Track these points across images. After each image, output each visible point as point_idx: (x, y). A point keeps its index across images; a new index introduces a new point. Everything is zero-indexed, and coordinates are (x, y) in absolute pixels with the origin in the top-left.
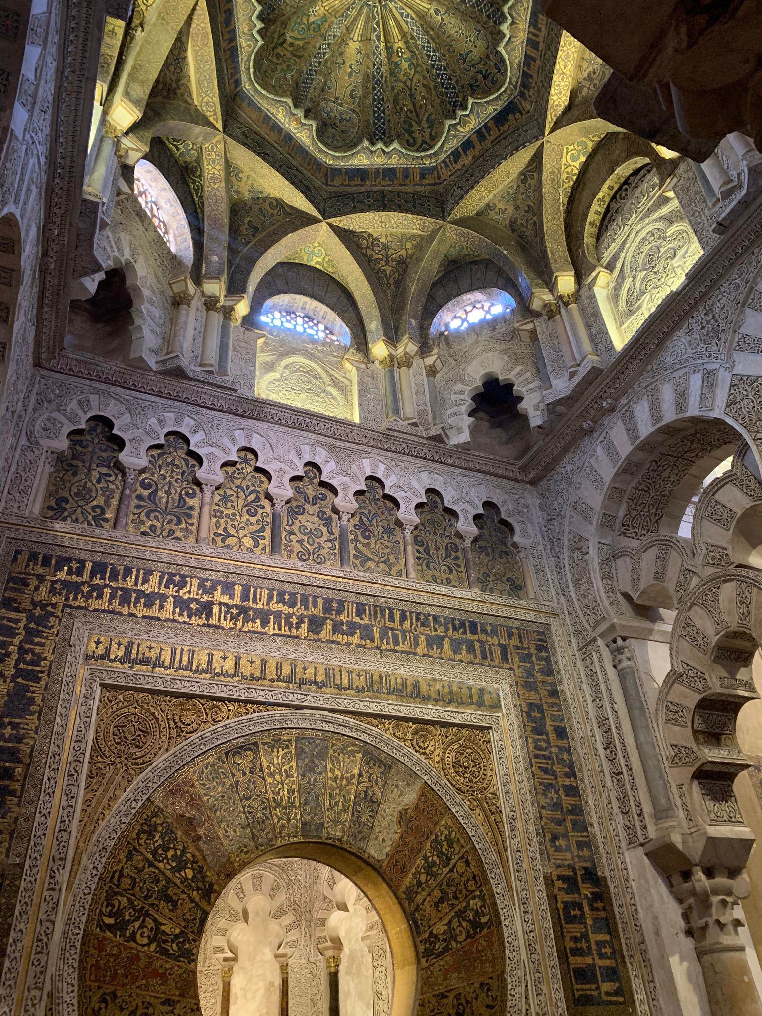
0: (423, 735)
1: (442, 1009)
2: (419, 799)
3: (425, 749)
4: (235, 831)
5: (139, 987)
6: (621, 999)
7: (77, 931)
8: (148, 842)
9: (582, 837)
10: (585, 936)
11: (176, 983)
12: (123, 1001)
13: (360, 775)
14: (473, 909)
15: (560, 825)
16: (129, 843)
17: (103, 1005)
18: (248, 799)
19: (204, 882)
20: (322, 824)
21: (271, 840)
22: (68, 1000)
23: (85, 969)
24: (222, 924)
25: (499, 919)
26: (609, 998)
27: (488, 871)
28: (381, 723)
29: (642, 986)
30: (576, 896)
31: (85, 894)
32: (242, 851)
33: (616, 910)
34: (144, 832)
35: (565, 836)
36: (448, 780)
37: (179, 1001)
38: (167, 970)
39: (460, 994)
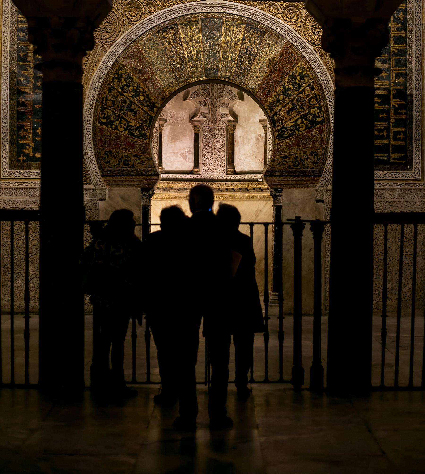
0: (290, 9)
1: (285, 163)
2: (284, 52)
3: (291, 18)
4: (165, 76)
5: (122, 149)
6: (405, 162)
7: (89, 125)
8: (119, 83)
9: (400, 70)
10: (387, 129)
11: (140, 148)
12: (115, 155)
13: (244, 39)
14: (312, 114)
15: (386, 64)
16: (109, 84)
17: (106, 156)
18: (172, 57)
19: (150, 102)
20: (217, 70)
21: (187, 80)
22: (90, 154)
23: (95, 141)
24: (225, 100)
25: (329, 119)
26: (395, 161)
27: (326, 93)
28: (260, 4)
29: (420, 156)
30: (387, 106)
31: (90, 109)
32: (170, 86)
33: (414, 114)
34: (116, 78)
35: (388, 70)
36: (306, 38)
37: (141, 156)
38: (134, 142)
39: (297, 157)
